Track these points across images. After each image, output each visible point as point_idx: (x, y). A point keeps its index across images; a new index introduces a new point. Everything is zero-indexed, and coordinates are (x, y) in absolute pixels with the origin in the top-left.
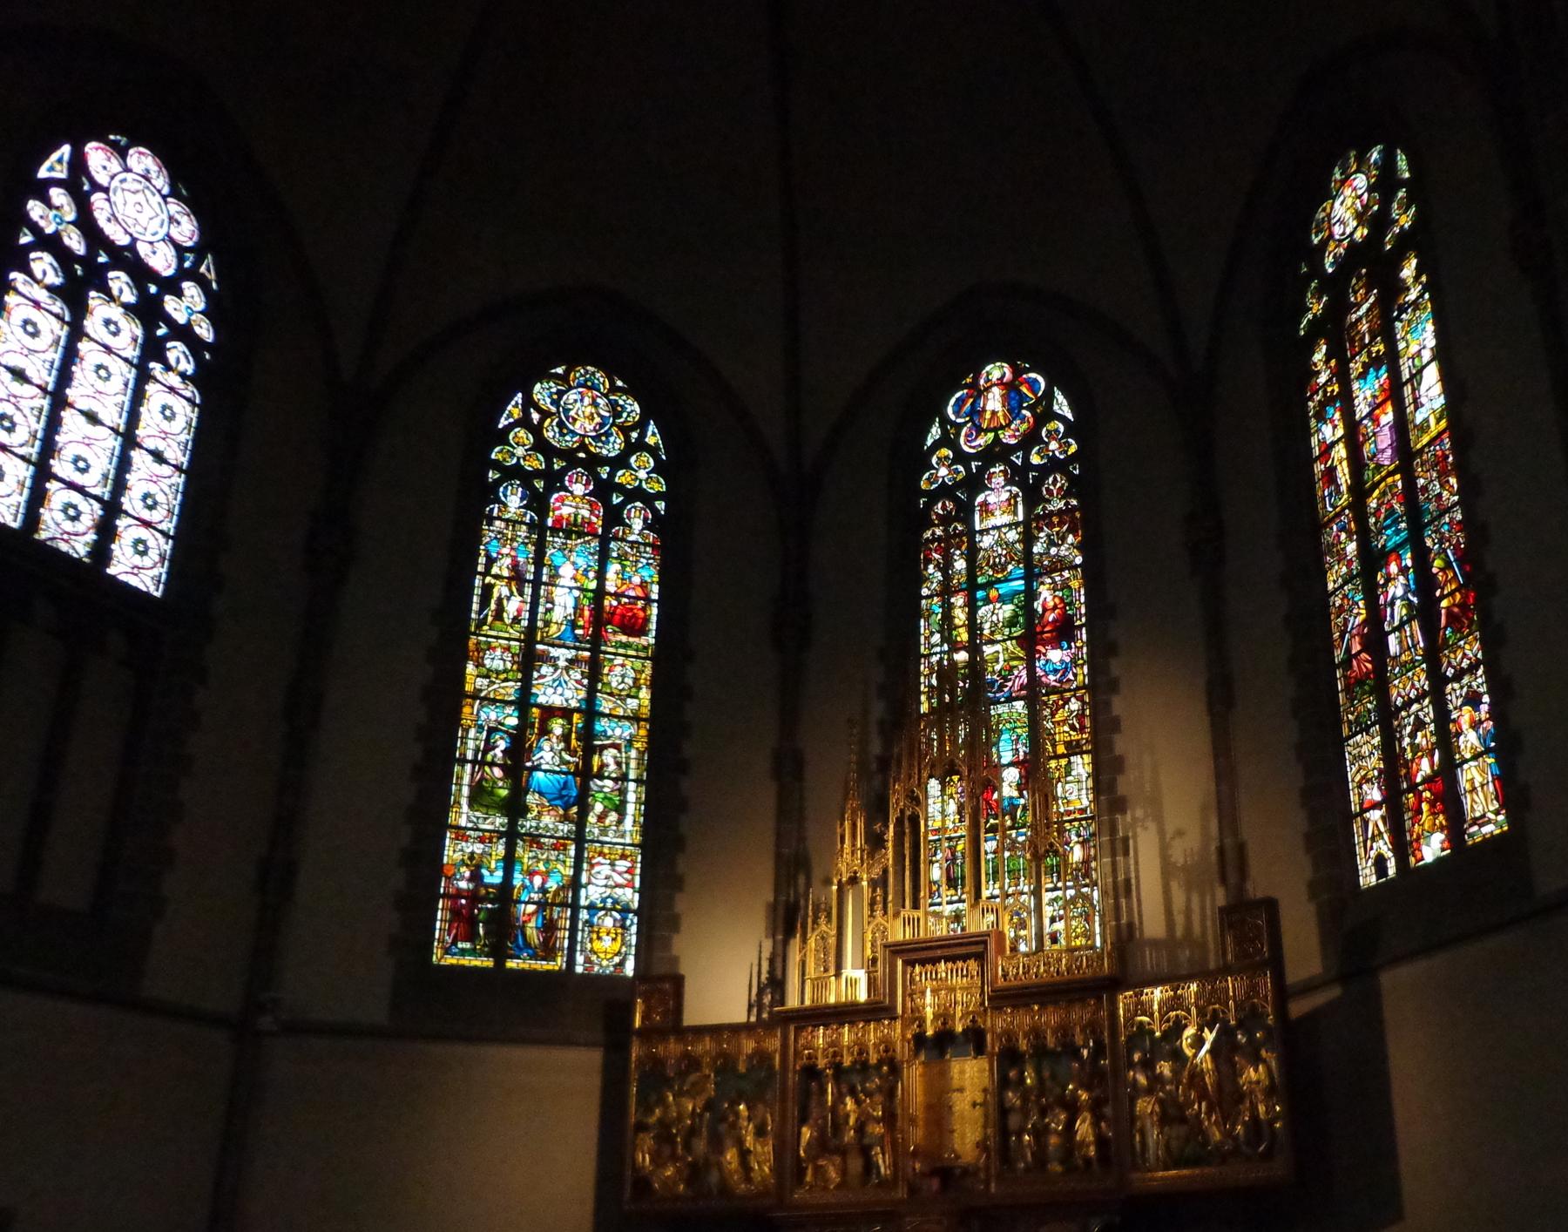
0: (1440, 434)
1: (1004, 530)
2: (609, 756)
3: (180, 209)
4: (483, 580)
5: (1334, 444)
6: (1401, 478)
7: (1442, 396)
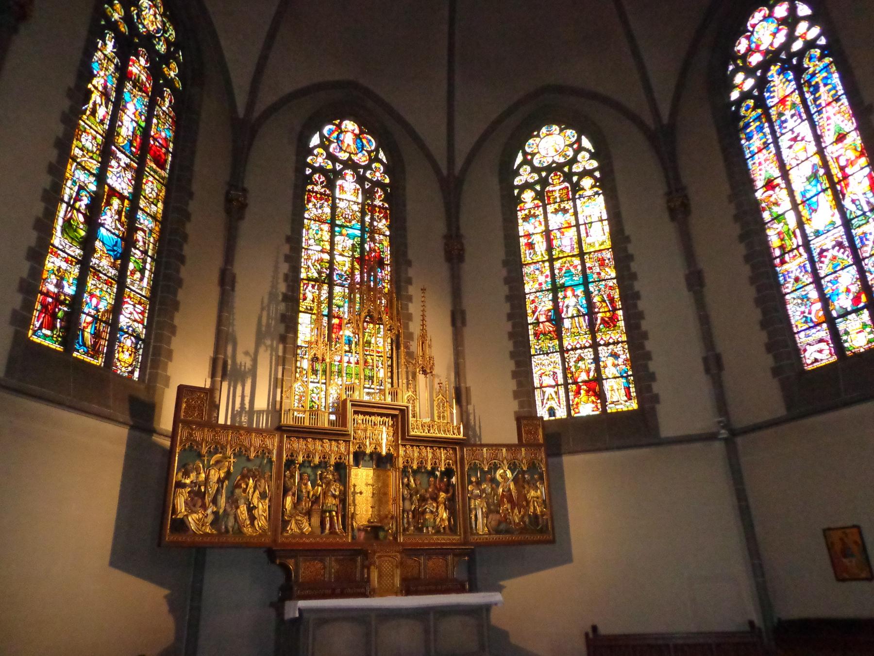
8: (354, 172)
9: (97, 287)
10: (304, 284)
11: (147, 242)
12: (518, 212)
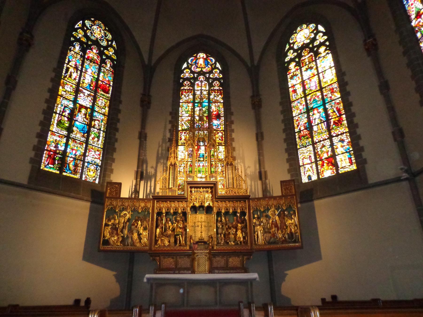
2: (97, 122)
4: (67, 65)
8: (204, 76)
9: (75, 146)
10: (181, 133)
11: (100, 125)
12: (288, 76)
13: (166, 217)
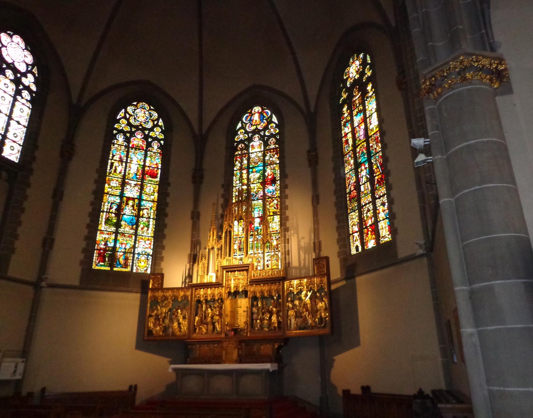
0: (377, 132)
1: (258, 153)
2: (145, 211)
3: (28, 53)
5: (348, 133)
6: (366, 143)
7: (377, 122)
8: (259, 135)
13: (206, 304)
